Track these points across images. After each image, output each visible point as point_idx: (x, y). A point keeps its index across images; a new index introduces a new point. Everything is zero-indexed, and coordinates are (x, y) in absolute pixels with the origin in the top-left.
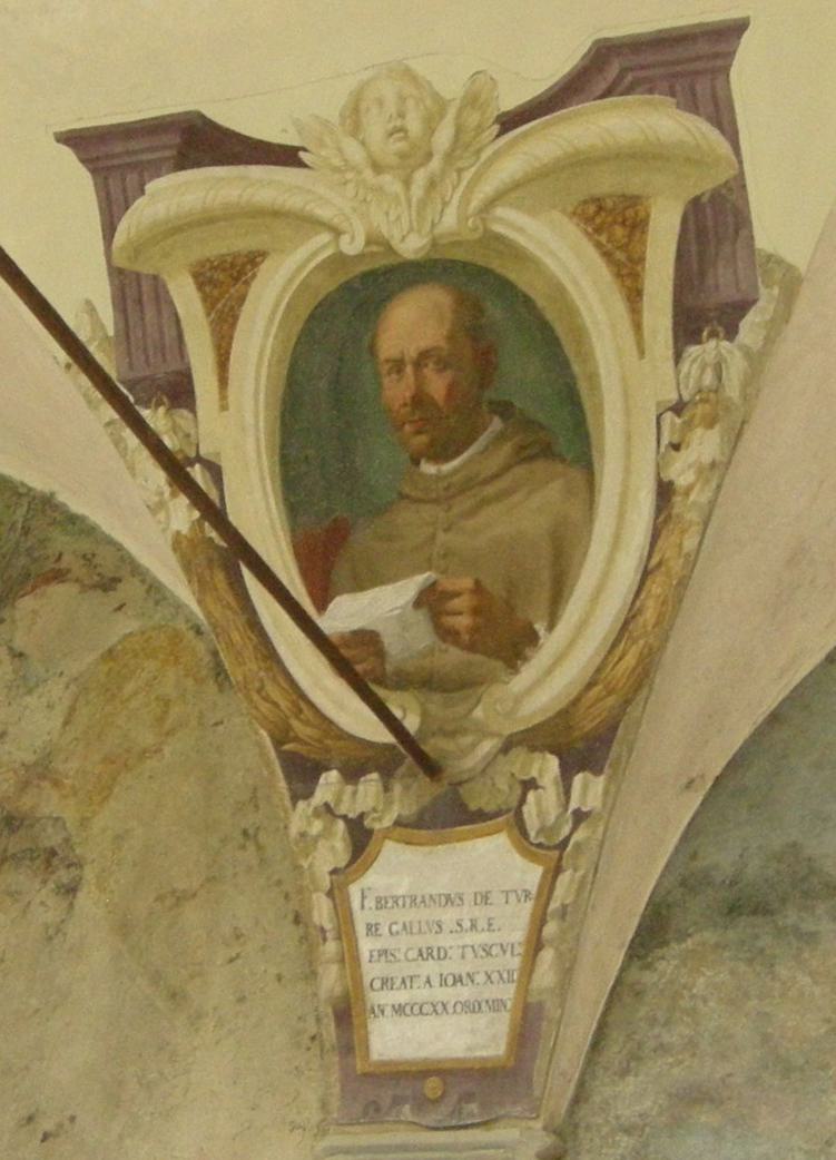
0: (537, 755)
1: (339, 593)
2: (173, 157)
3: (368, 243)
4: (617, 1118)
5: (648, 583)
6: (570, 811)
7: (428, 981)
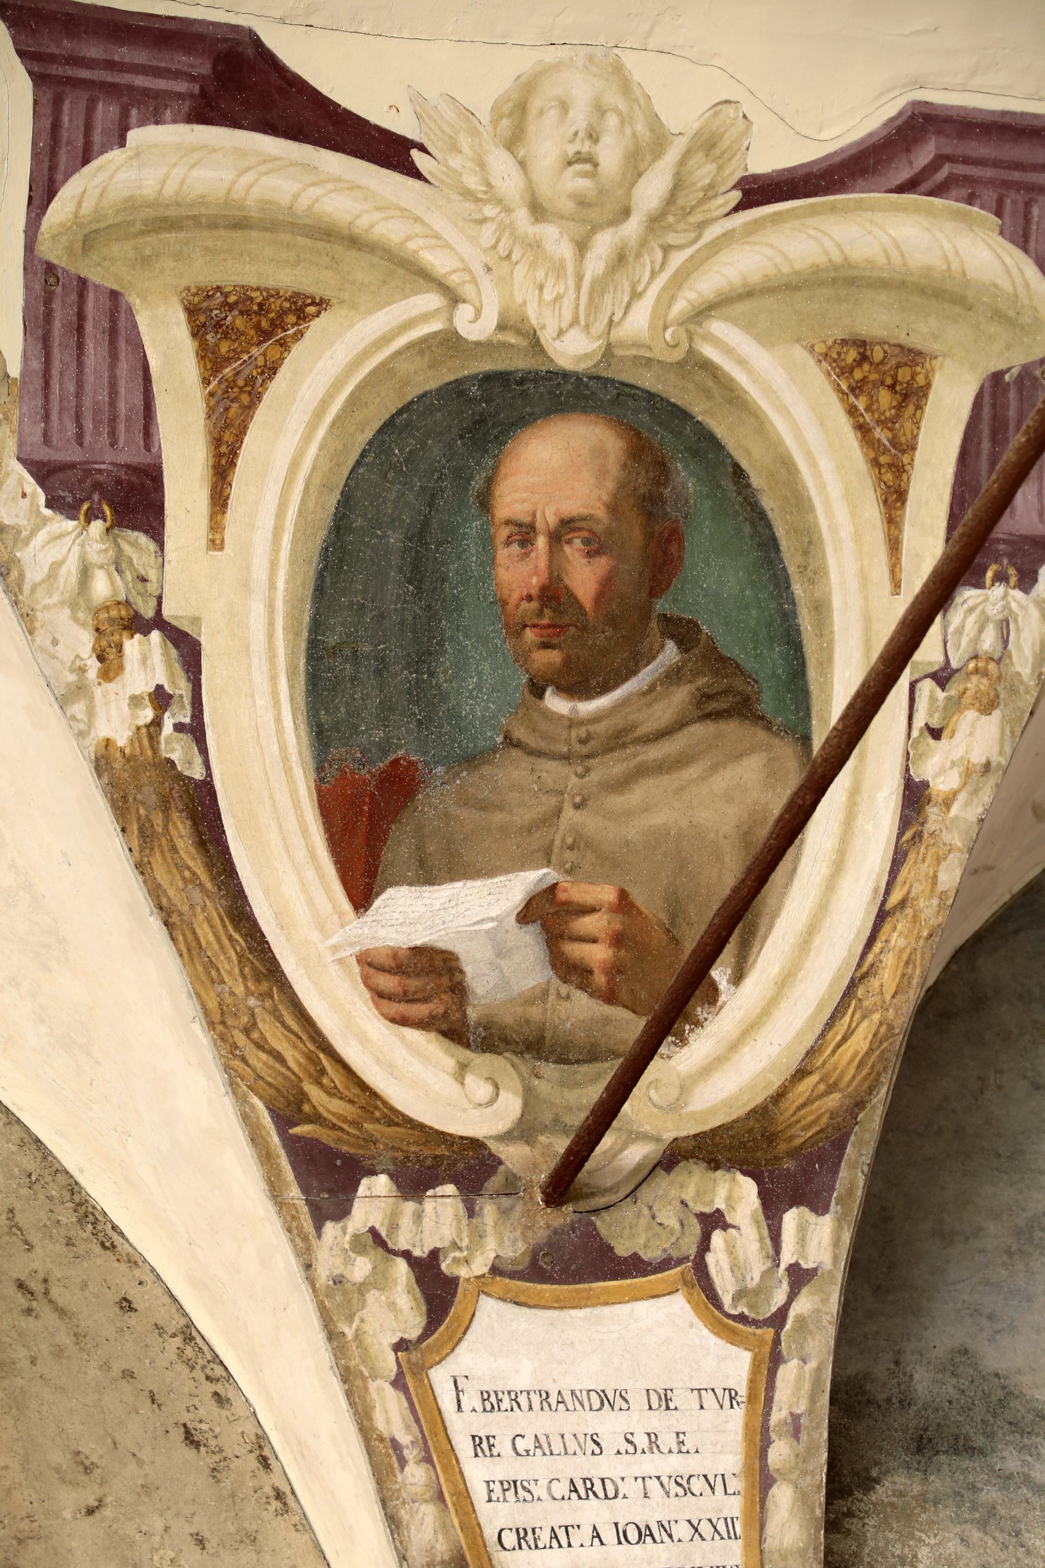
0: (719, 1173)
2: (192, 96)
3: (502, 327)
5: (887, 927)
6: (783, 1266)
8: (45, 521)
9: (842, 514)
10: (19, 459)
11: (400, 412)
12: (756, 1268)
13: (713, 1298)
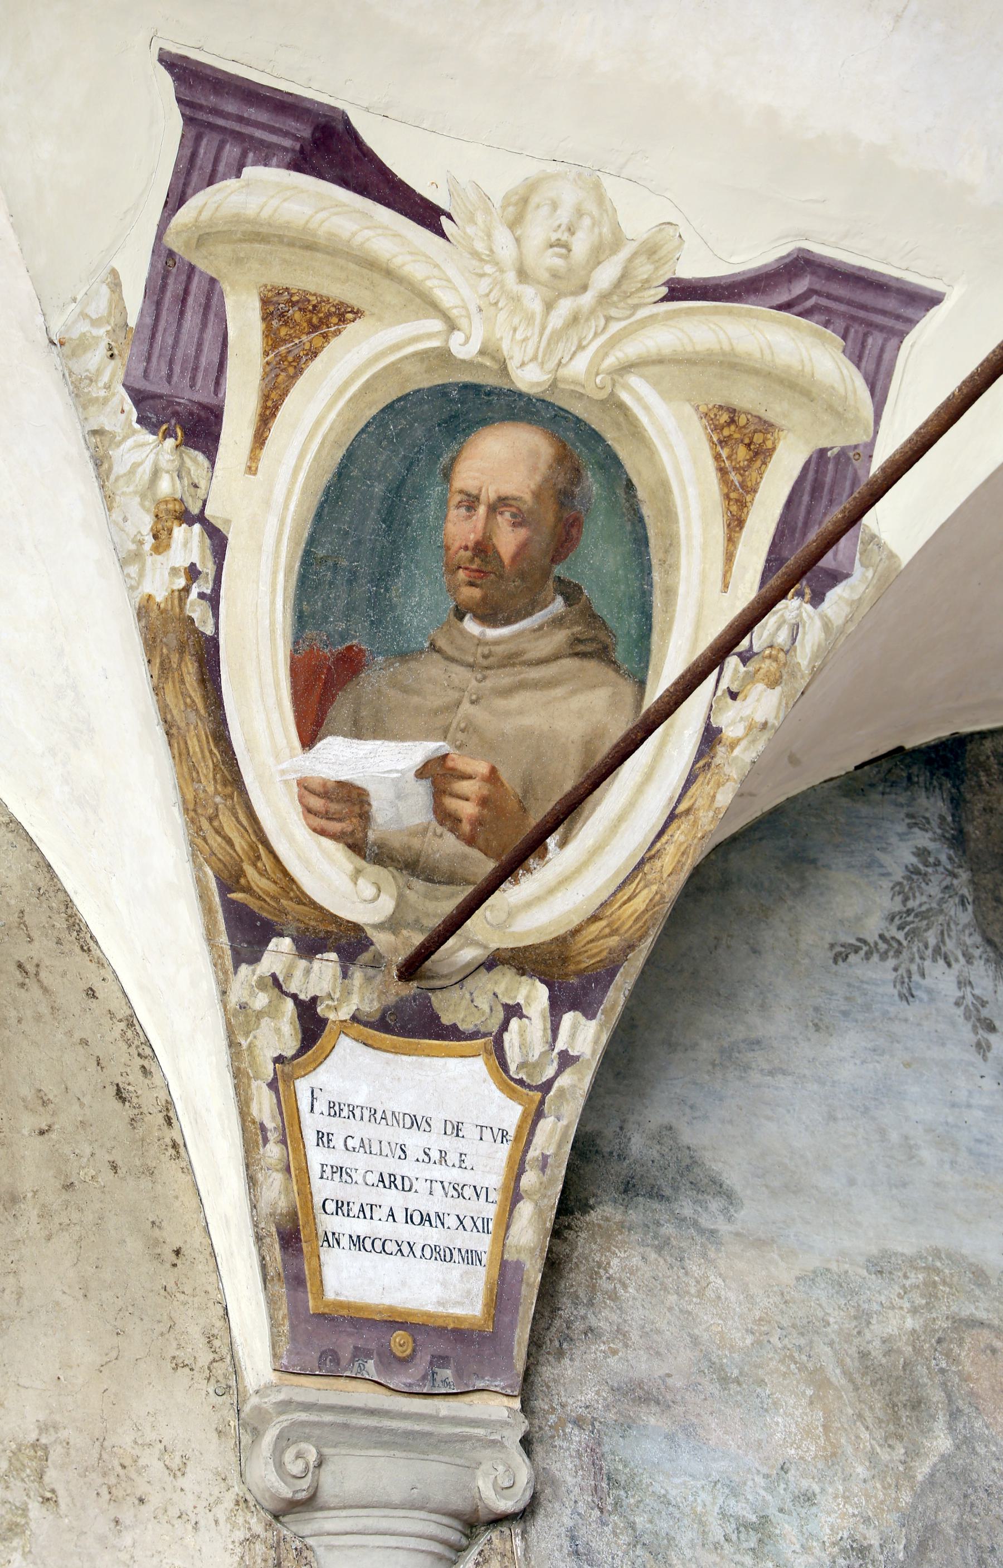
0: (524, 978)
1: (331, 734)
2: (293, 150)
3: (482, 352)
5: (674, 826)
6: (556, 1051)
8: (134, 432)
9: (697, 529)
10: (124, 385)
11: (399, 400)
12: (538, 1048)
13: (504, 1065)
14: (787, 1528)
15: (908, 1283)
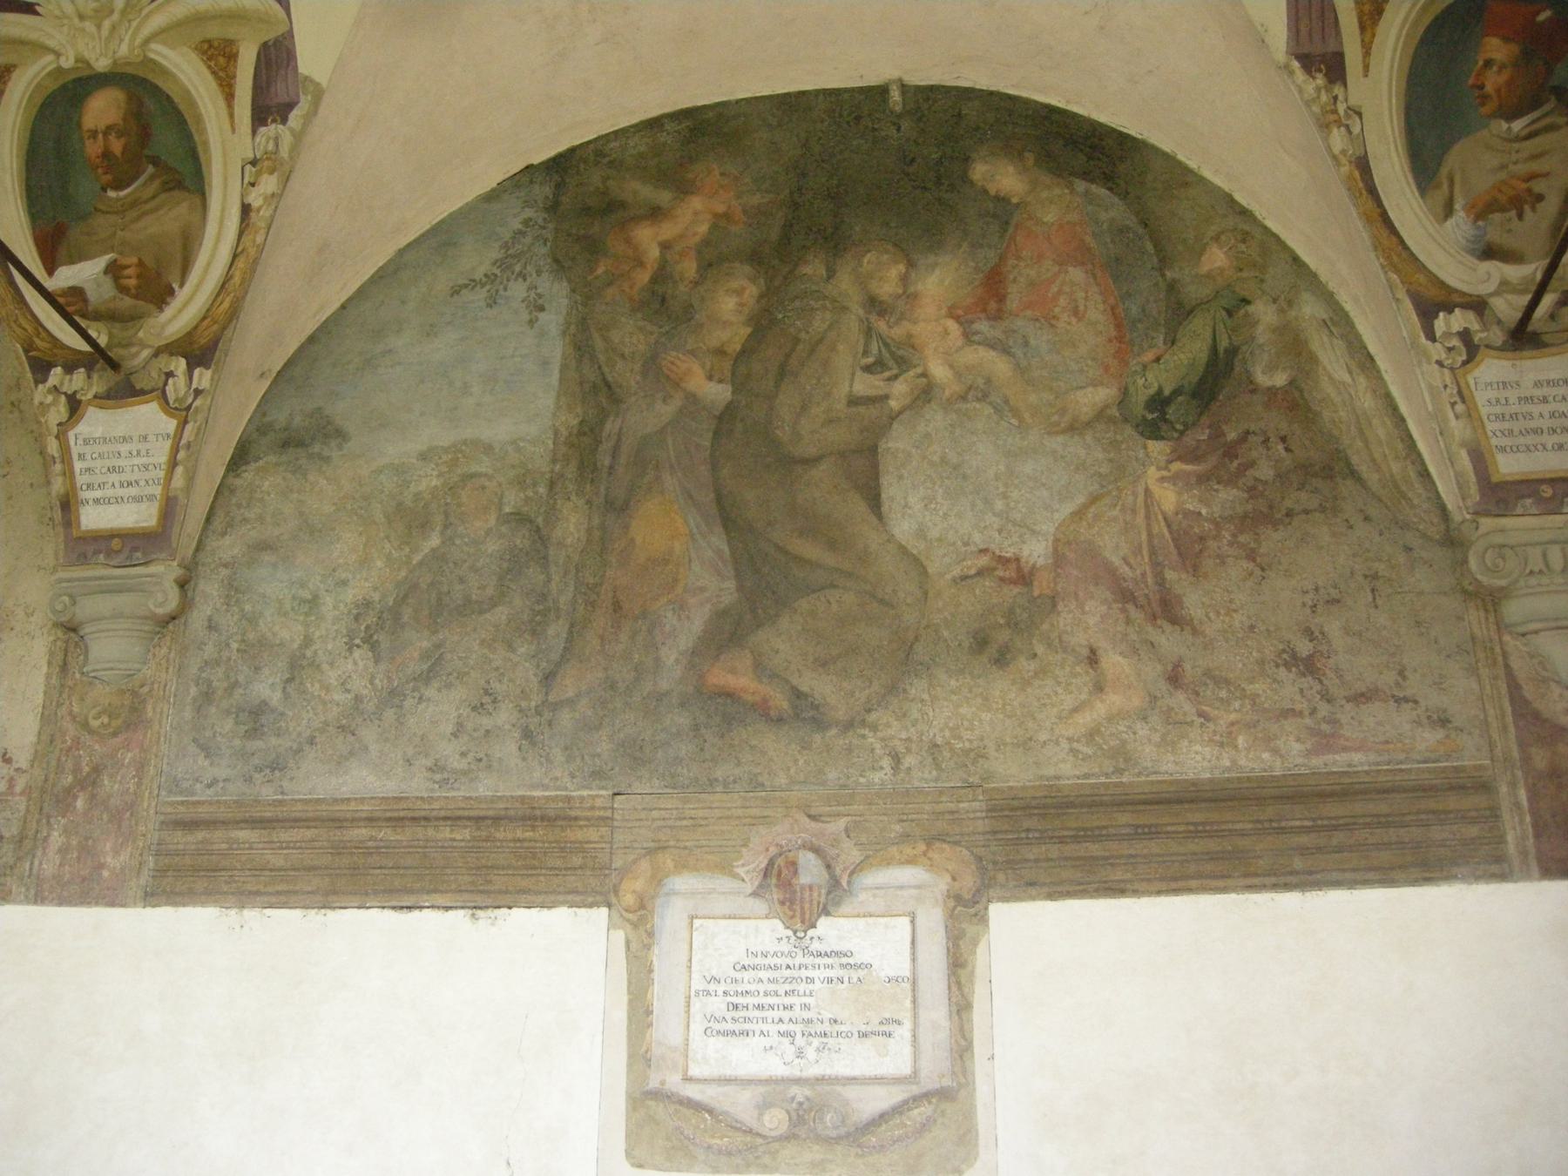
0: (174, 358)
1: (60, 266)
4: (220, 559)
7: (113, 485)
14: (329, 600)
15: (440, 461)
